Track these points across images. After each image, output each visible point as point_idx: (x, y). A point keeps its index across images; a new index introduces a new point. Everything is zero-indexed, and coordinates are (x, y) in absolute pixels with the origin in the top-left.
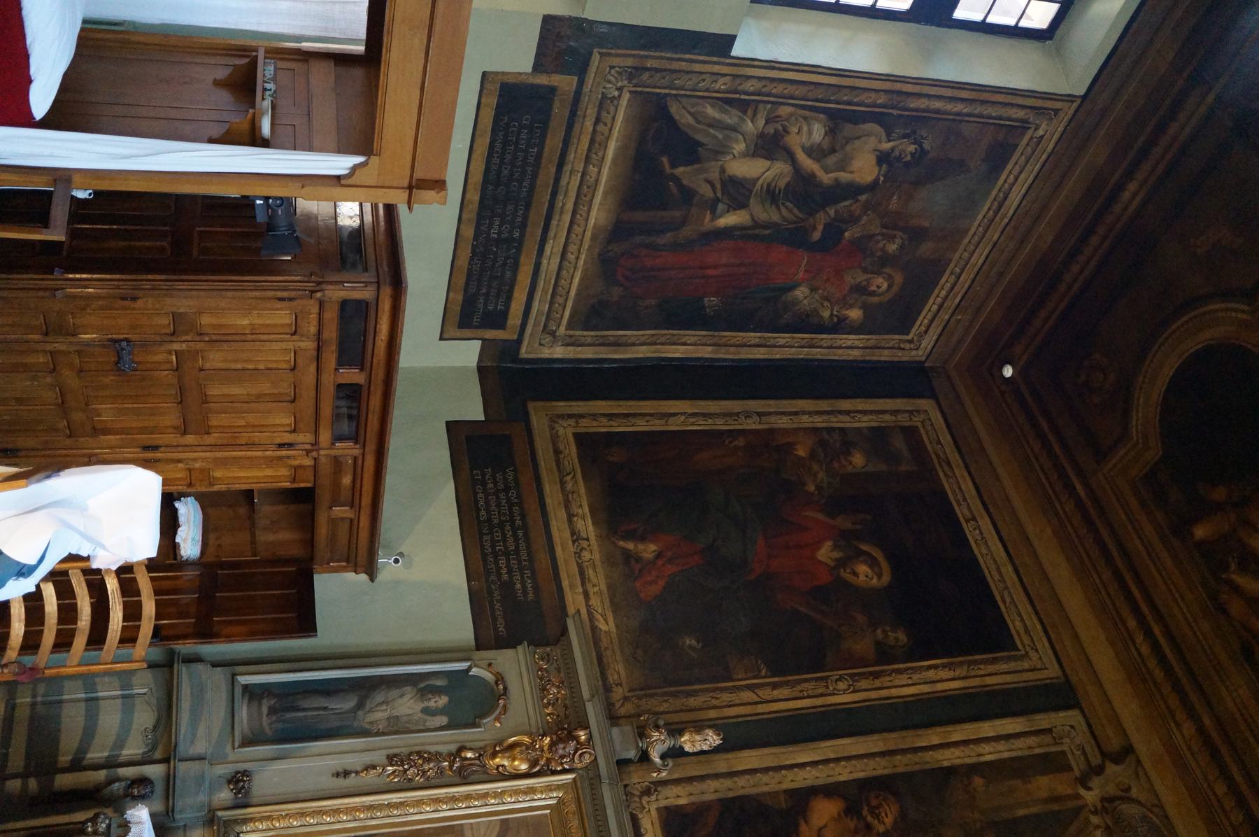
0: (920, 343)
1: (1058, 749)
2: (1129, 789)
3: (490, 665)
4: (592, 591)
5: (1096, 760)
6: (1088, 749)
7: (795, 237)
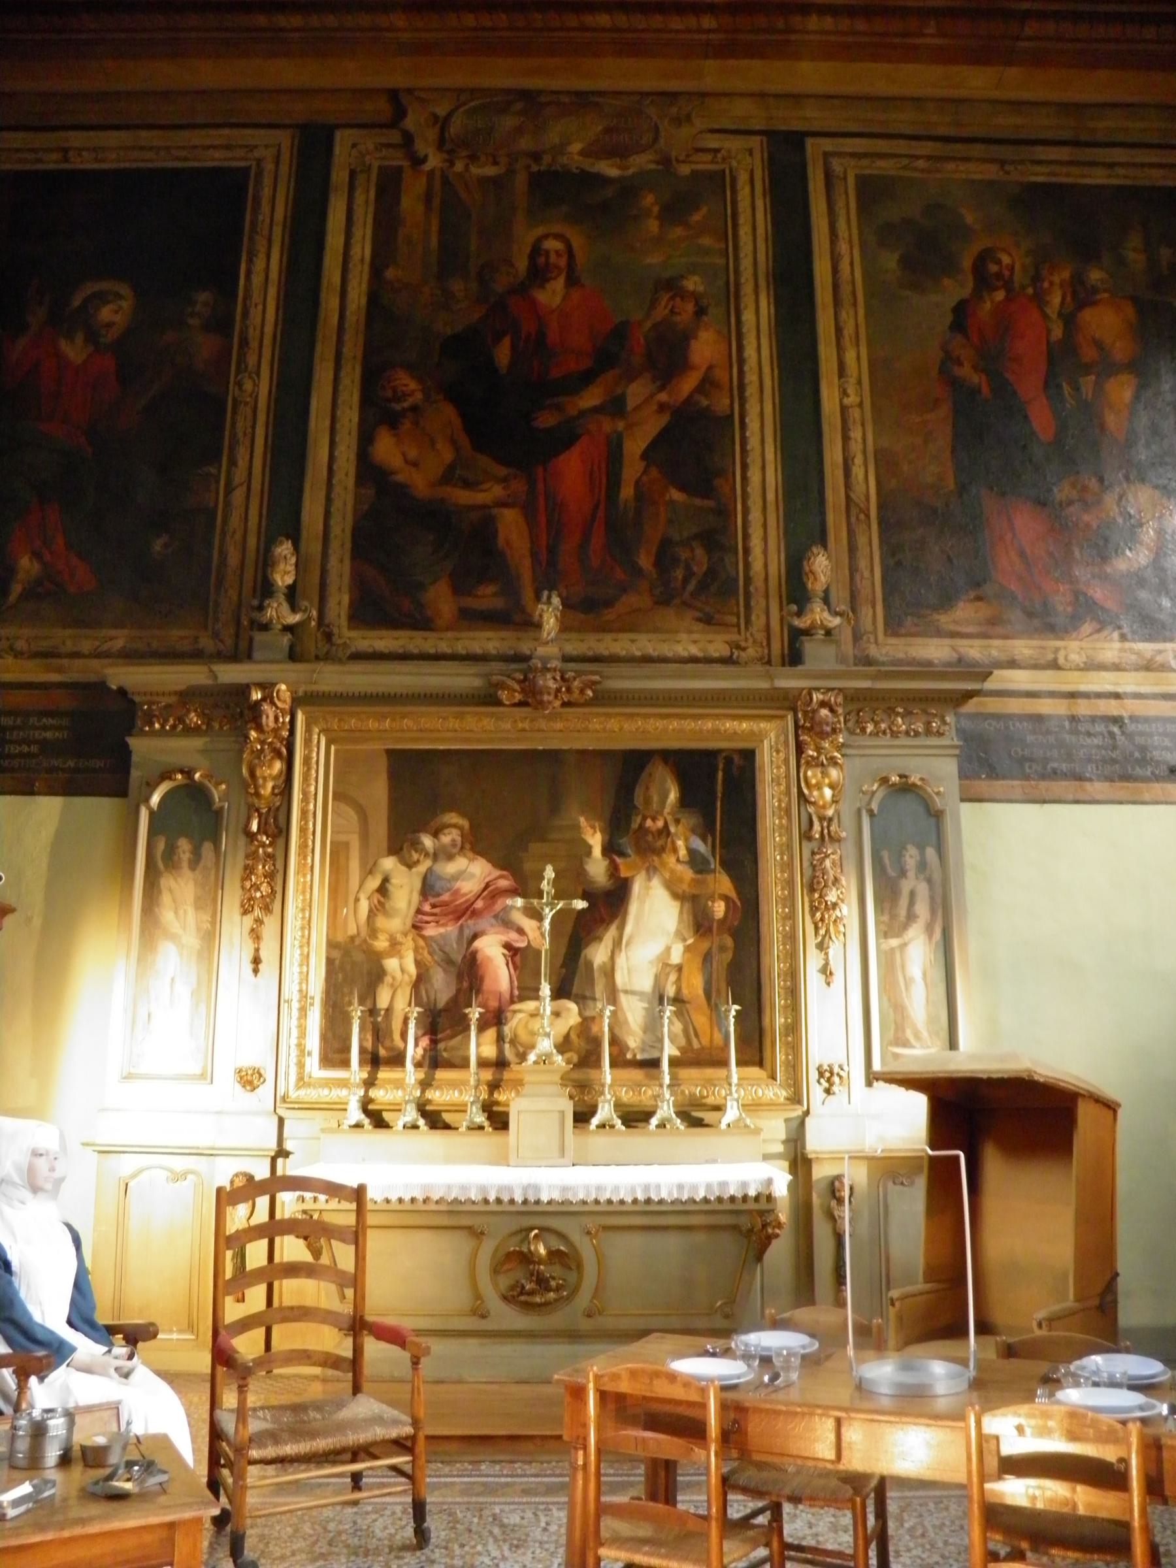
1: (375, 172)
2: (435, 117)
3: (148, 784)
4: (69, 646)
5: (395, 137)
6: (384, 140)
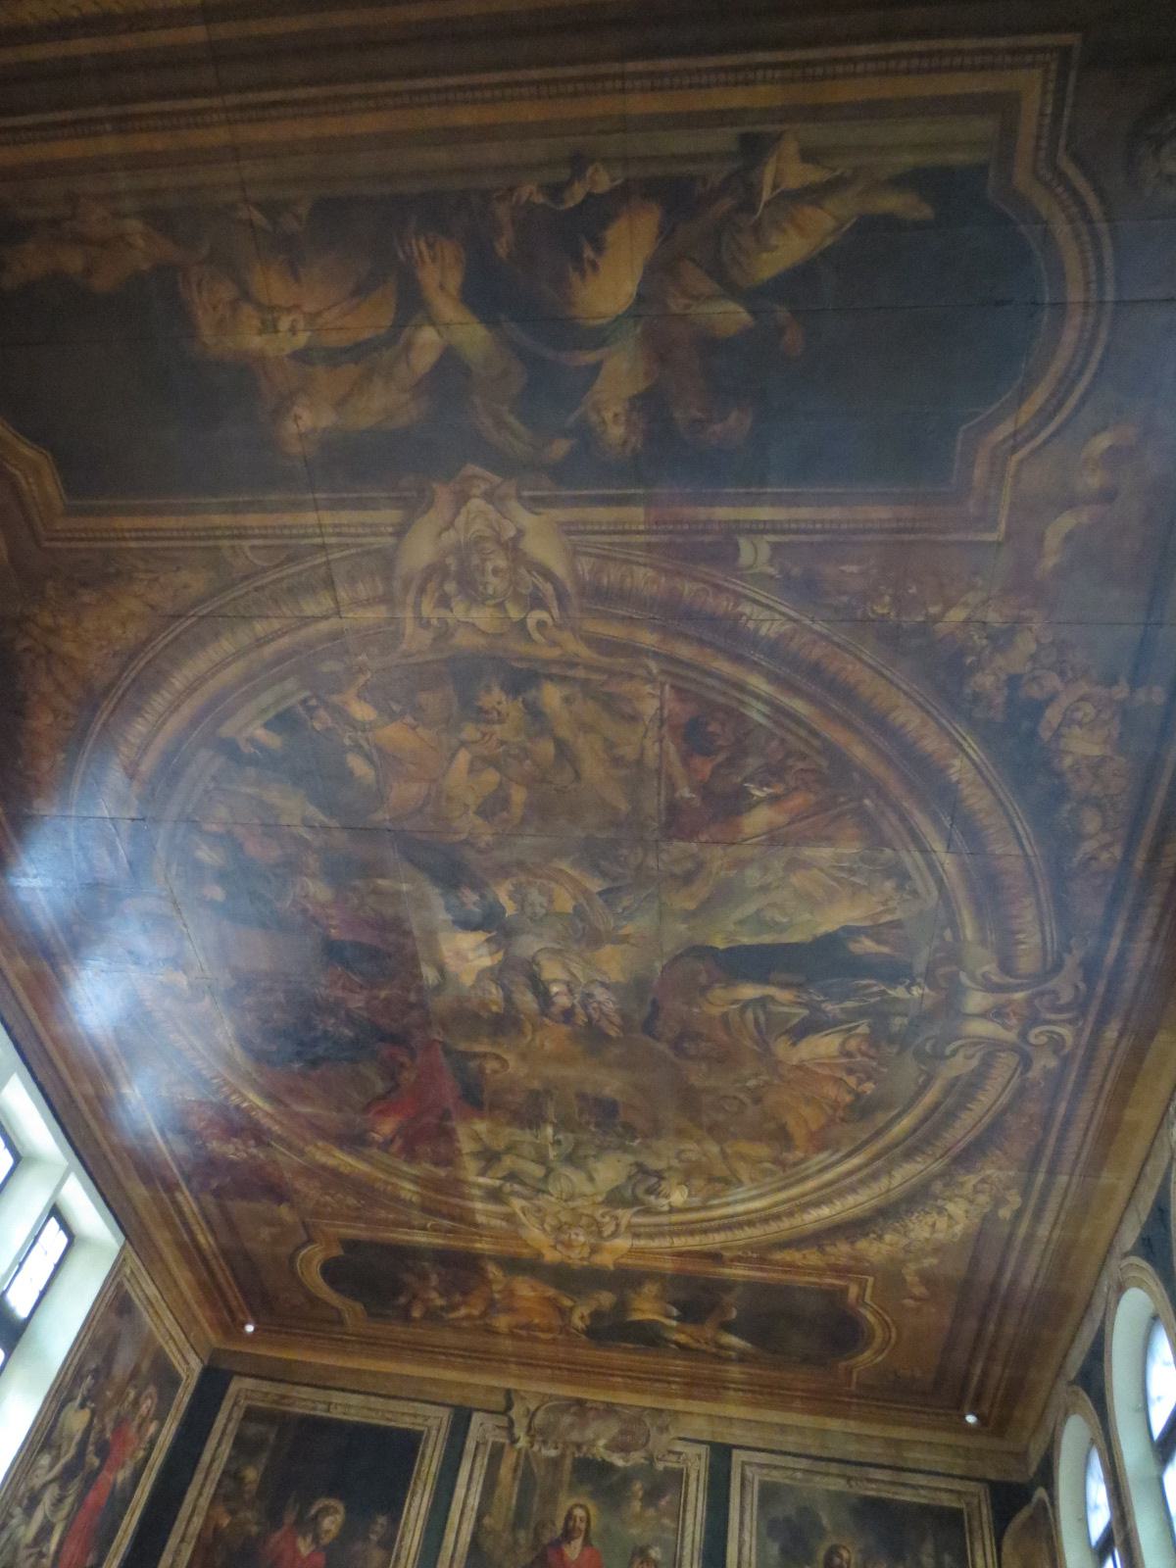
0: (190, 1368)
1: (490, 1444)
2: (528, 1410)
5: (503, 1421)
7: (91, 1478)
